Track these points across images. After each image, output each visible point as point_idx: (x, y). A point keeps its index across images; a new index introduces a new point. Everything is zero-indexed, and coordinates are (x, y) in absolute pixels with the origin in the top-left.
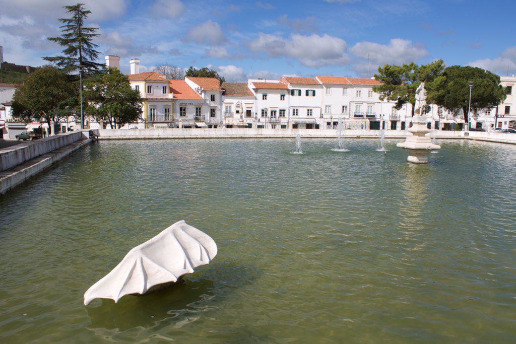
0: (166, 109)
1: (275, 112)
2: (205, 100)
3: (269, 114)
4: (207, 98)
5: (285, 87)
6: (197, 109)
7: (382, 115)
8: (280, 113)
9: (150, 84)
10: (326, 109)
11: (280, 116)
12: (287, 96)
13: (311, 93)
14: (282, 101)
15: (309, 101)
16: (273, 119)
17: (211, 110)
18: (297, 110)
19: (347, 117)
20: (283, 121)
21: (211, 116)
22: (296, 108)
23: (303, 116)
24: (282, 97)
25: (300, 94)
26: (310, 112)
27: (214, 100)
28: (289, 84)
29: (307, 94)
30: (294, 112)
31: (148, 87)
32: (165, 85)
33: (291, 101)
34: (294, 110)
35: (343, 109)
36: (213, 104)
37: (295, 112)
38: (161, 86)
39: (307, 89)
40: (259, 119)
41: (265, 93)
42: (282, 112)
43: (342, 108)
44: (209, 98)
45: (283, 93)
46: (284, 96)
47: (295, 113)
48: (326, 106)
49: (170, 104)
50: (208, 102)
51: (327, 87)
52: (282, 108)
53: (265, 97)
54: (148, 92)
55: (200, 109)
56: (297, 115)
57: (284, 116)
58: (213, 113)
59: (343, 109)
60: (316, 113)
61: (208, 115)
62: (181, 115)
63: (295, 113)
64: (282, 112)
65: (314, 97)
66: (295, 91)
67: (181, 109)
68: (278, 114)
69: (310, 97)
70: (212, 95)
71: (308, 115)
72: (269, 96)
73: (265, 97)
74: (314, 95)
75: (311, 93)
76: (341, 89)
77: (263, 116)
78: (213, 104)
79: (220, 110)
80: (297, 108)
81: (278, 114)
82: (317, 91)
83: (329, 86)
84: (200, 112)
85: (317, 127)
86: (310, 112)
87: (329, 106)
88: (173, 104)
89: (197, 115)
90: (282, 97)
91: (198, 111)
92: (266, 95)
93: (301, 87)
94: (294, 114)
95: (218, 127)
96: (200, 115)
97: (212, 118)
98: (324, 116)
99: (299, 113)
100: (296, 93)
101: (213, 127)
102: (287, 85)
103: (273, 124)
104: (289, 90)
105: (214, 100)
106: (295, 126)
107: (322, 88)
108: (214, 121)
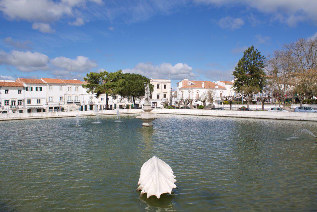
0: (40, 103)
1: (15, 102)
3: (10, 103)
5: (21, 85)
7: (84, 102)
8: (19, 102)
10: (49, 99)
11: (19, 104)
12: (22, 91)
13: (39, 89)
14: (20, 94)
15: (38, 94)
16: (13, 107)
18: (30, 100)
19: (63, 103)
20: (20, 107)
24: (20, 92)
25: (32, 90)
26: (39, 101)
28: (24, 83)
29: (37, 90)
30: (28, 102)
33: (25, 95)
34: (28, 100)
35: (60, 99)
37: (29, 102)
39: (36, 86)
40: (3, 107)
41: (7, 89)
42: (20, 102)
43: (59, 98)
45: (20, 89)
46: (21, 91)
47: (39, 102)
48: (50, 97)
51: (50, 85)
52: (20, 99)
53: (6, 92)
56: (30, 103)
59: (60, 99)
60: (43, 102)
63: (39, 102)
65: (41, 92)
66: (29, 88)
68: (17, 103)
69: (39, 92)
71: (38, 103)
72: (10, 91)
73: (6, 92)
74: (41, 90)
75: (39, 89)
76: (59, 87)
77: (6, 104)
80: (30, 99)
81: (17, 103)
82: (43, 87)
83: (50, 84)
85: (44, 111)
86: (39, 101)
87: (51, 97)
90: (20, 92)
92: (7, 91)
93: (33, 85)
94: (28, 103)
98: (49, 104)
100: (29, 89)
102: (23, 84)
103: (14, 110)
104: (24, 87)
106: (29, 111)
107: (47, 85)
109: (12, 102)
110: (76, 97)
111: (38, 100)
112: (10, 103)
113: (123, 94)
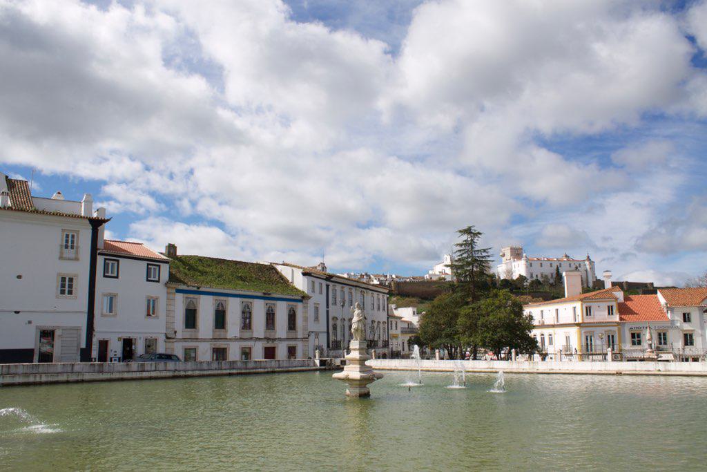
2: (673, 322)
4: (676, 318)
6: (660, 334)
9: (588, 304)
17: (686, 335)
21: (686, 344)
27: (689, 321)
31: (587, 308)
32: (610, 304)
36: (687, 327)
38: (604, 305)
44: (678, 319)
49: (616, 329)
50: (678, 324)
54: (587, 315)
55: (664, 334)
58: (688, 340)
61: (678, 344)
62: (634, 343)
67: (633, 336)
70: (684, 314)
78: (687, 327)
79: (702, 335)
84: (665, 339)
88: (619, 330)
89: (660, 343)
91: (663, 337)
95: (700, 360)
96: (665, 343)
97: (688, 348)
101: (690, 359)
105: (689, 321)
108: (689, 351)
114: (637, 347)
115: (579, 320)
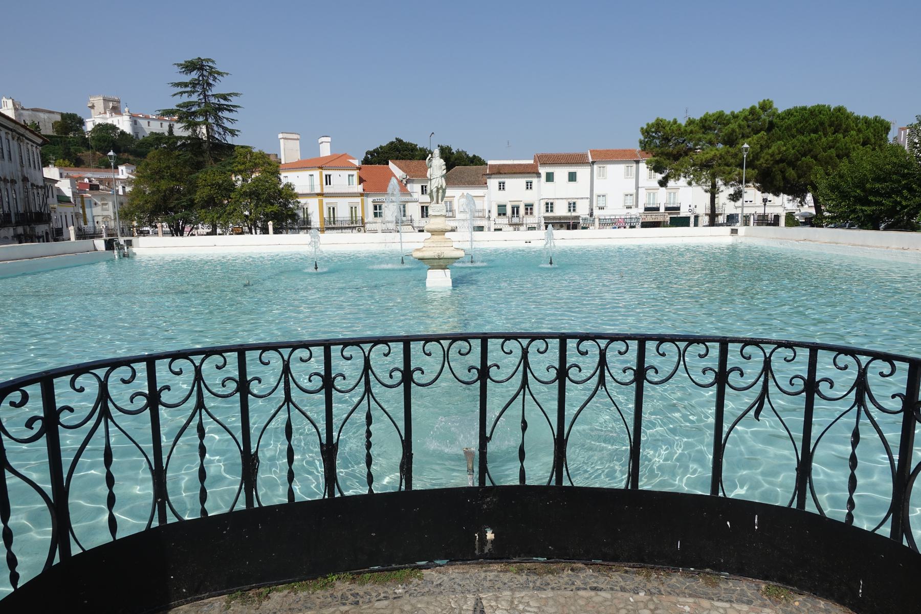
1: (518, 208)
3: (509, 211)
8: (527, 209)
11: (527, 213)
14: (529, 191)
16: (515, 220)
18: (552, 204)
20: (530, 220)
22: (549, 201)
23: (561, 210)
26: (572, 206)
30: (547, 207)
33: (541, 191)
34: (547, 204)
37: (549, 206)
42: (529, 208)
49: (358, 200)
52: (529, 201)
53: (502, 186)
57: (531, 213)
62: (376, 215)
64: (529, 208)
67: (375, 208)
68: (522, 211)
73: (502, 186)
81: (522, 211)
86: (572, 206)
88: (362, 200)
90: (529, 186)
94: (547, 211)
99: (555, 209)
109: (513, 208)
110: (650, 194)
111: (570, 204)
112: (509, 211)
113: (770, 183)
114: (378, 219)
115: (318, 191)
